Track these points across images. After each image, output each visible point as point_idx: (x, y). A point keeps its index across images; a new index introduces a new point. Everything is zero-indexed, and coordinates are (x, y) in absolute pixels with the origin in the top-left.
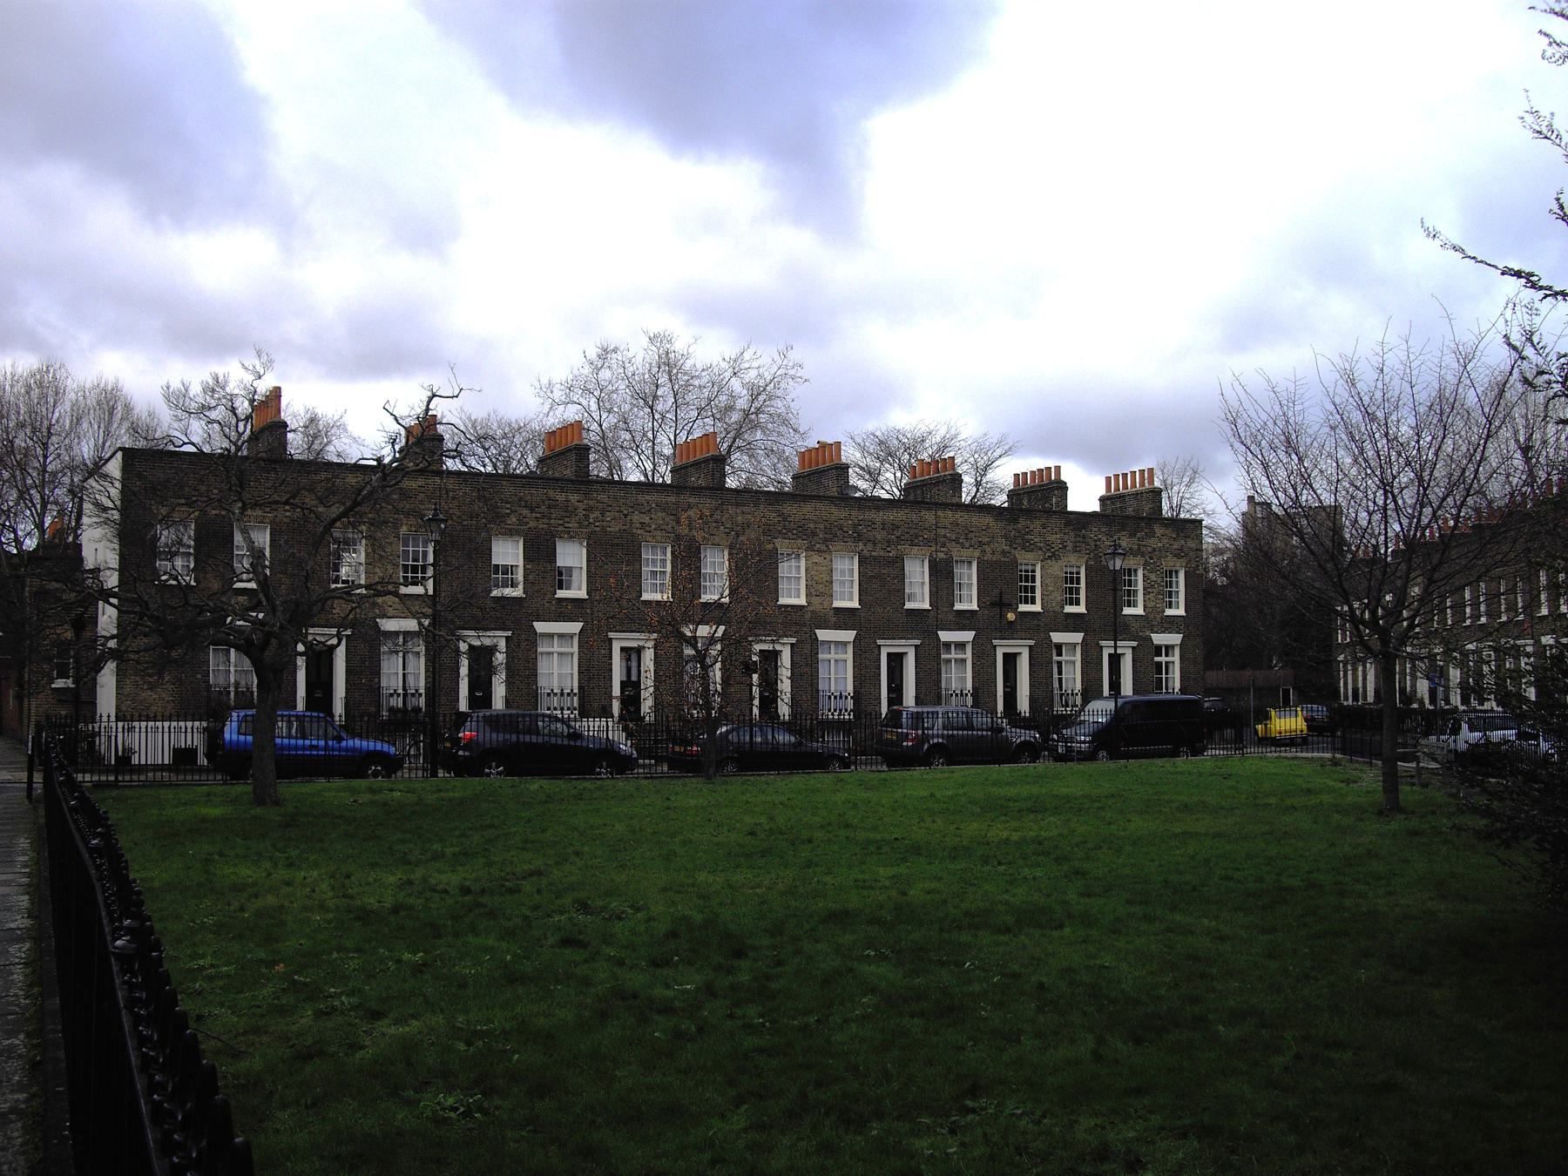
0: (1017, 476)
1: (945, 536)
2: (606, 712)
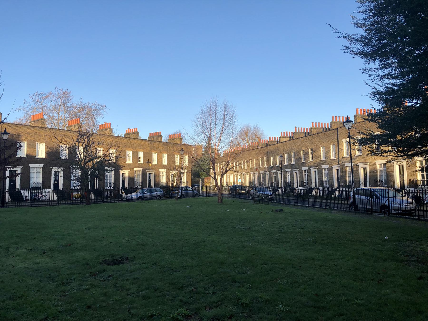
0: (150, 134)
1: (136, 146)
2: (50, 188)
